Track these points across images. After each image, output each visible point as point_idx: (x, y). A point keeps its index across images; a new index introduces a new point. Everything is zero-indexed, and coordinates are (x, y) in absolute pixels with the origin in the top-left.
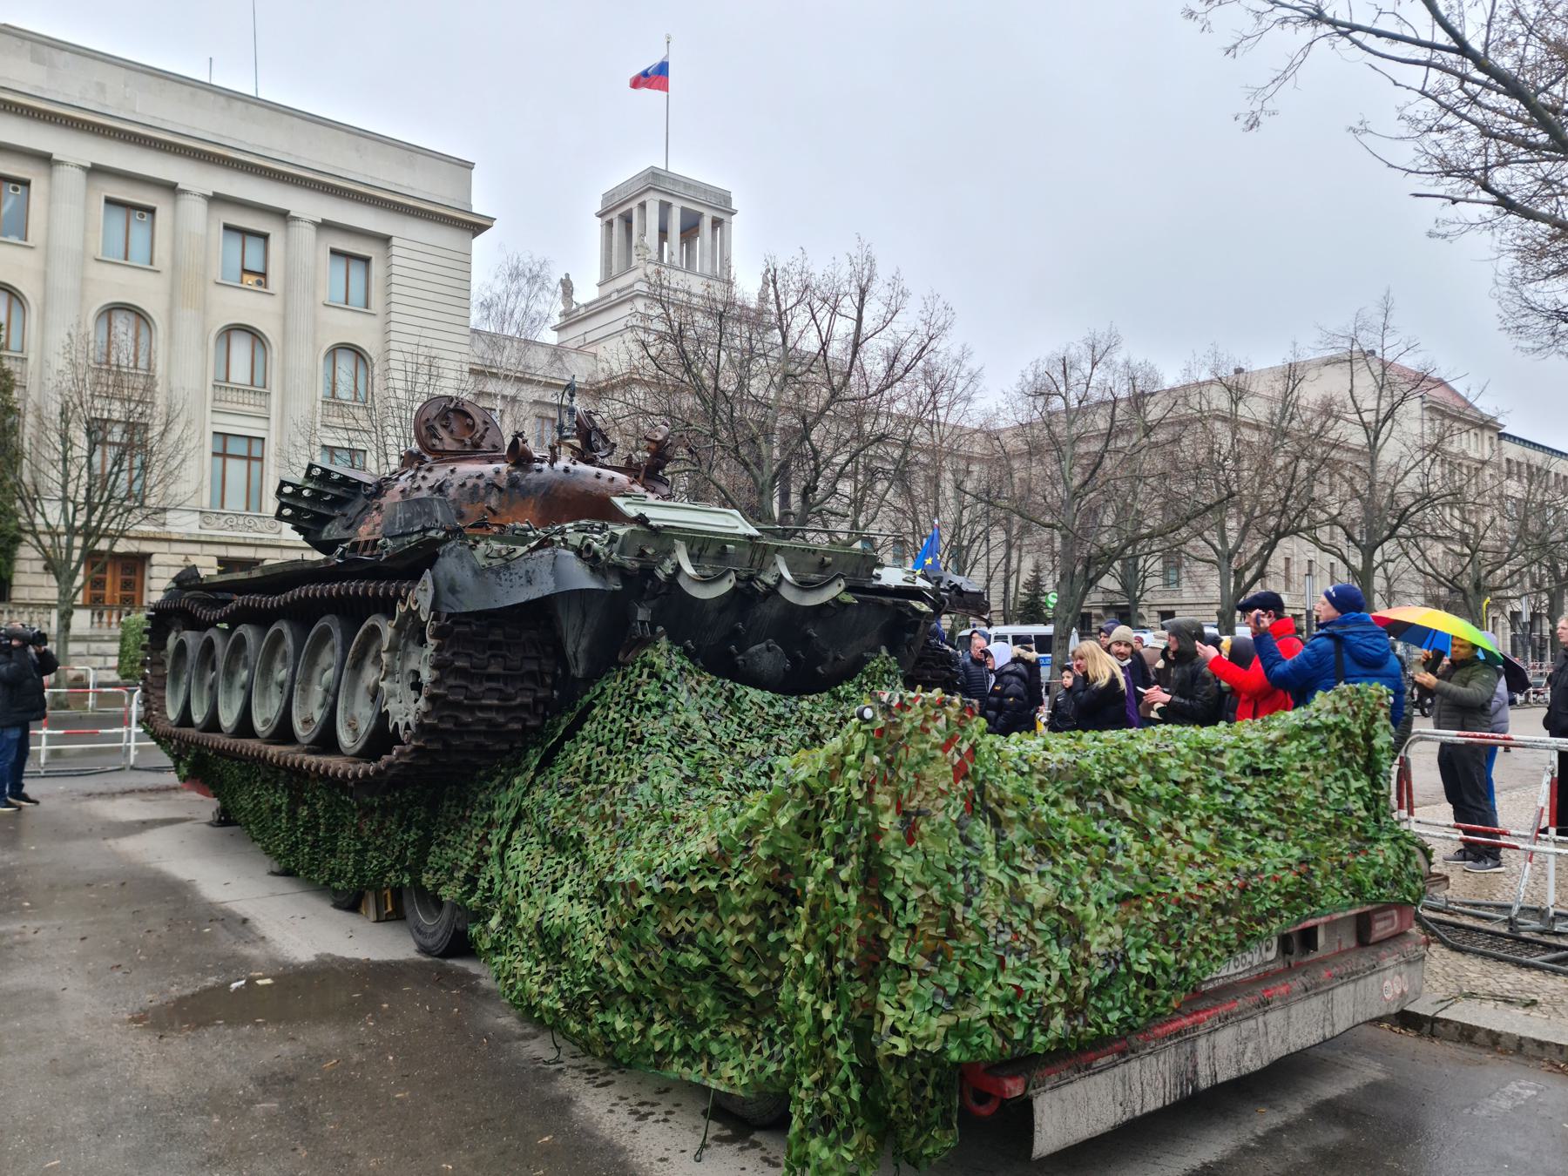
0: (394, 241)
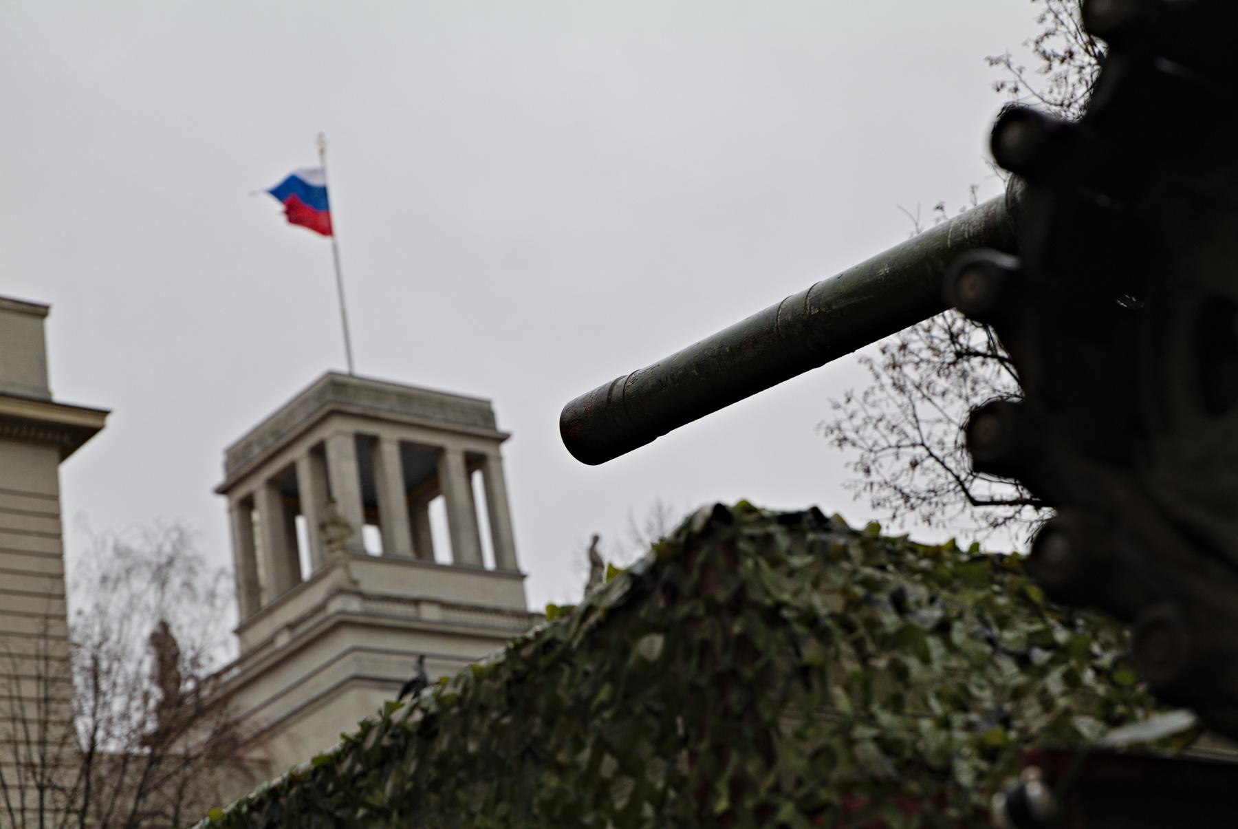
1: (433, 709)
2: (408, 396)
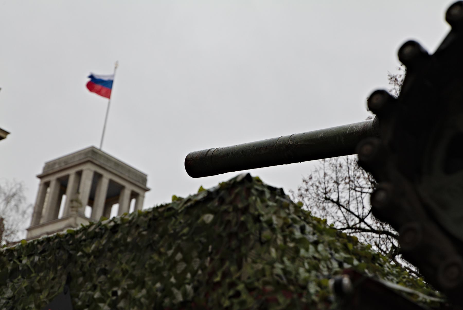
1: (119, 222)
2: (118, 164)
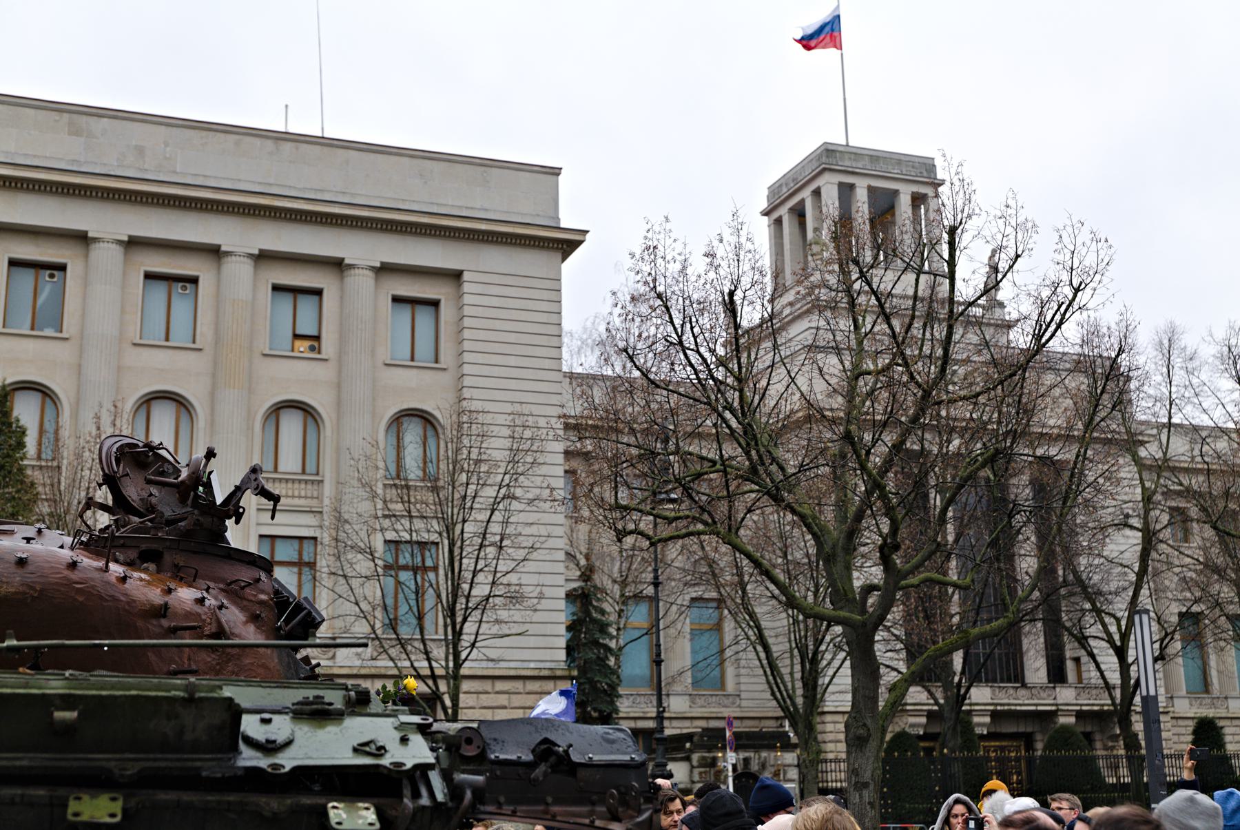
0: (466, 276)
2: (876, 157)
